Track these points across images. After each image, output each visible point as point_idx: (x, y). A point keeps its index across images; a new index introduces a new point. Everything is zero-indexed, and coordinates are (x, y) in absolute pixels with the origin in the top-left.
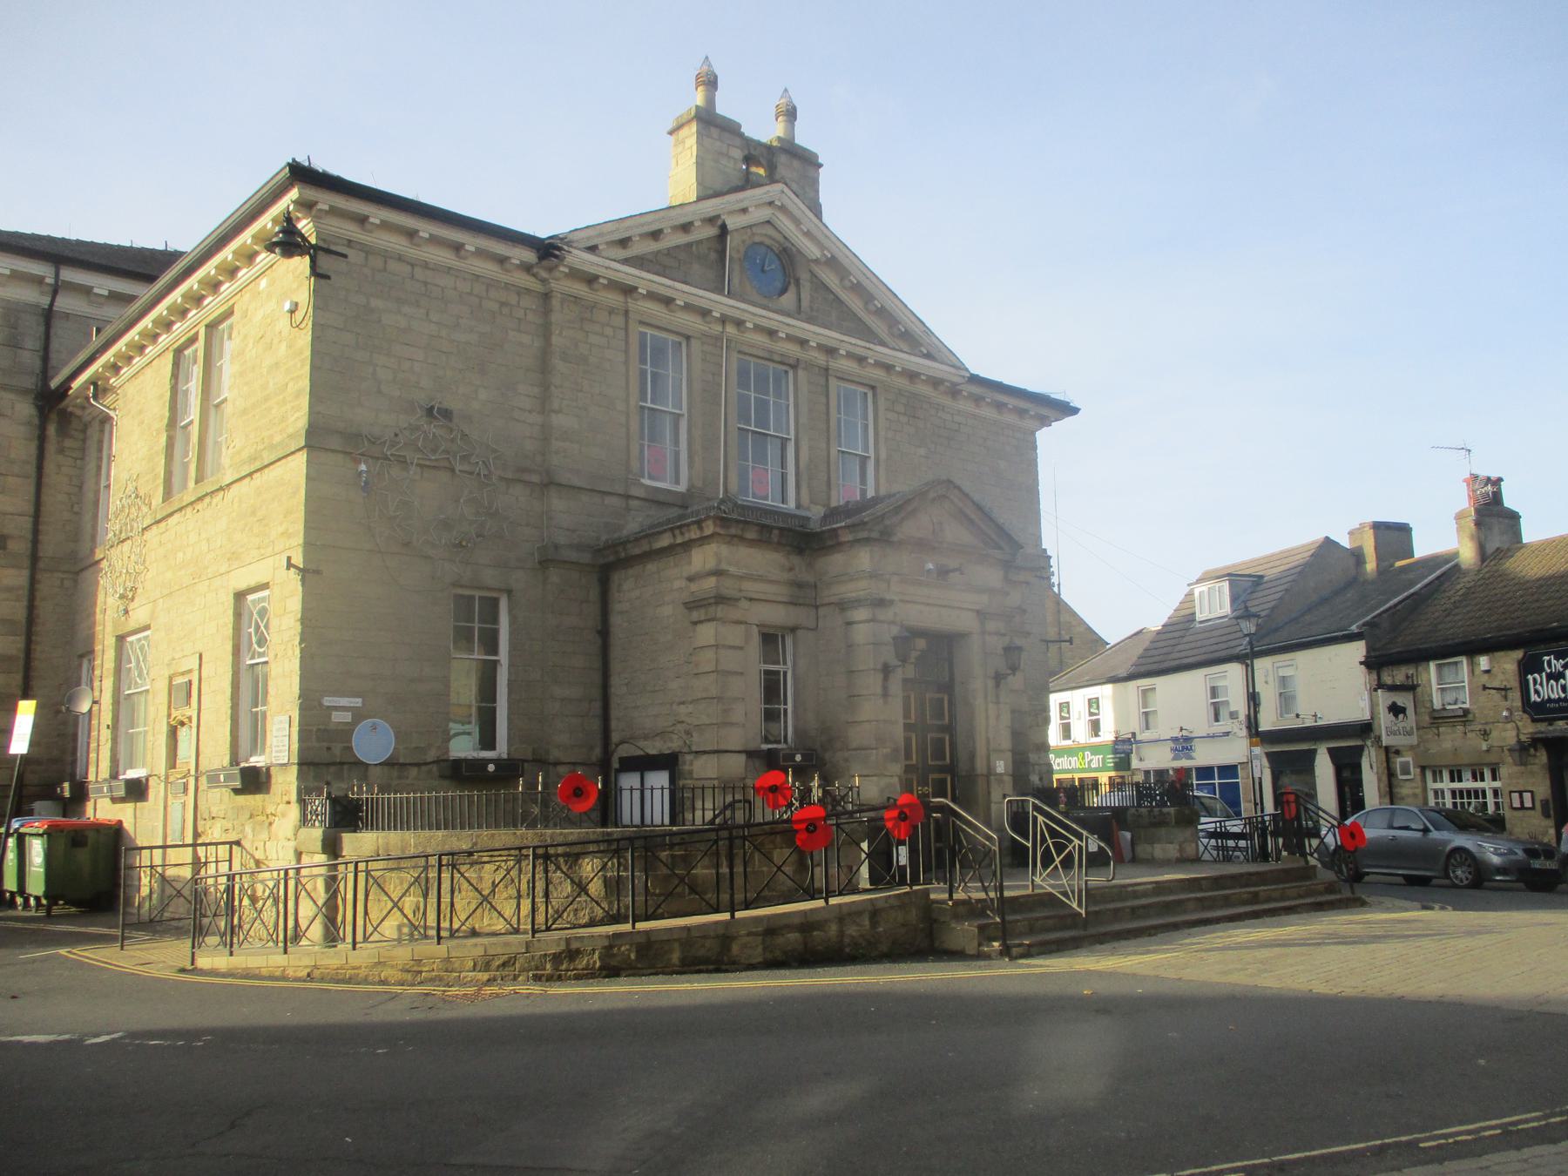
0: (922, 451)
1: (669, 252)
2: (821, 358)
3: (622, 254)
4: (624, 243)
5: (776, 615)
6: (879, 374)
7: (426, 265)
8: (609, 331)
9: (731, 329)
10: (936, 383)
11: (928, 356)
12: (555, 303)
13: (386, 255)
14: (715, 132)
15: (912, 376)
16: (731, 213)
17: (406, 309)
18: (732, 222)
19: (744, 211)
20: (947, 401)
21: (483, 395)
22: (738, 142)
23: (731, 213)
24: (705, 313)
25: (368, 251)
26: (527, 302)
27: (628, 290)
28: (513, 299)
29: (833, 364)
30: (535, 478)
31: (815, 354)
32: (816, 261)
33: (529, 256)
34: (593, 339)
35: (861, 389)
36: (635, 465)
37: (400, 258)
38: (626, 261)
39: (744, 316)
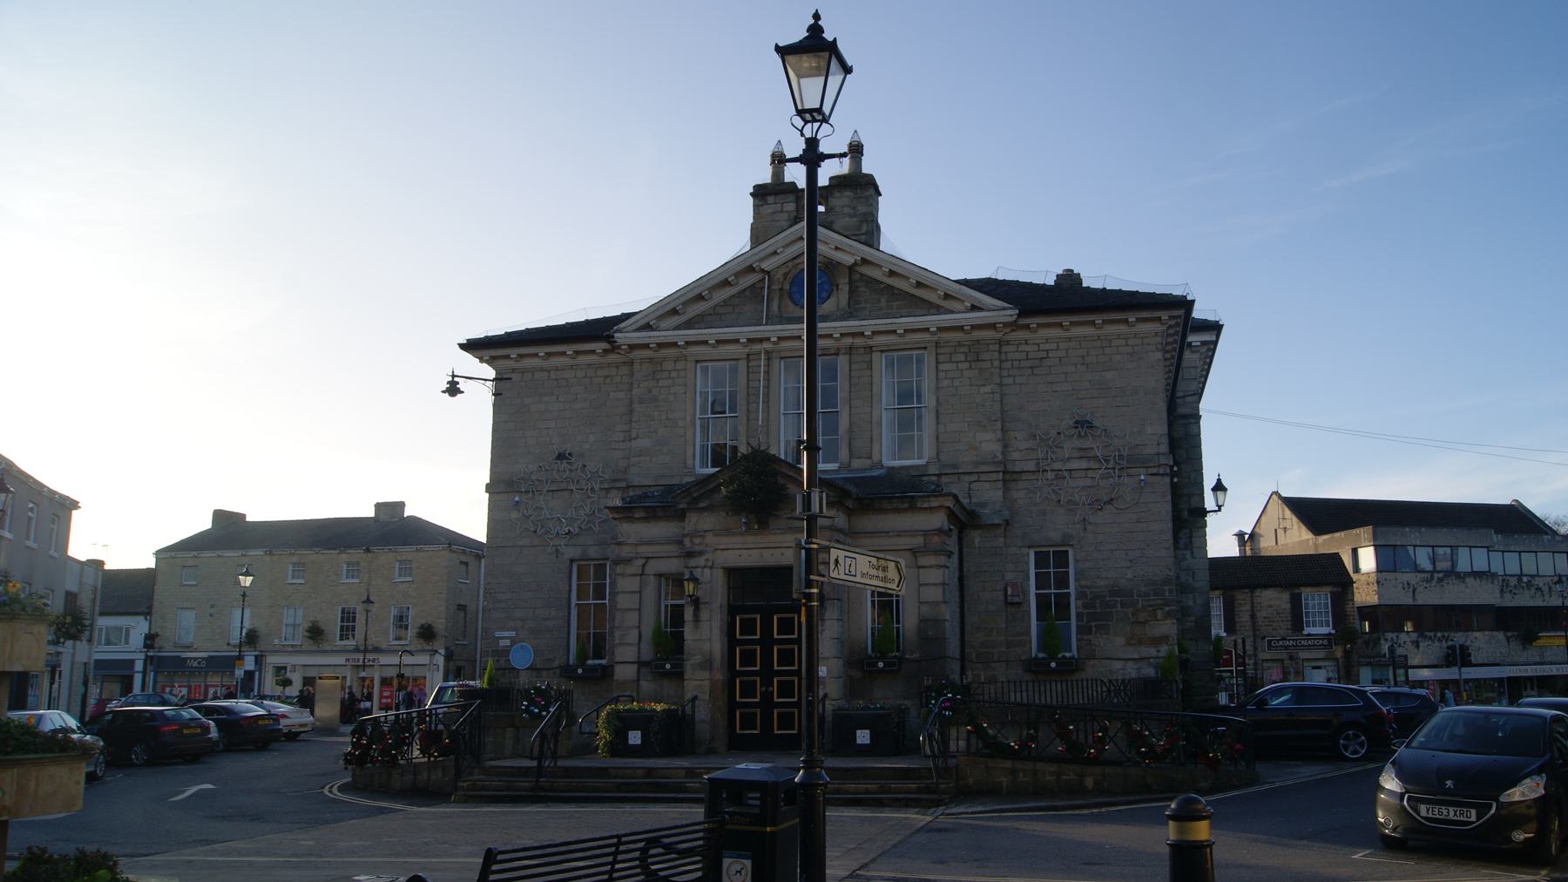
0: (988, 389)
1: (725, 303)
2: (859, 341)
3: (676, 320)
4: (674, 312)
5: (672, 566)
6: (926, 336)
7: (557, 369)
8: (674, 374)
9: (766, 345)
10: (993, 326)
11: (974, 308)
12: (637, 367)
13: (533, 370)
14: (771, 199)
15: (961, 328)
16: (762, 259)
17: (546, 399)
18: (766, 265)
19: (775, 253)
20: (1021, 335)
21: (592, 438)
22: (791, 197)
23: (762, 259)
24: (737, 341)
25: (523, 371)
26: (624, 370)
27: (675, 345)
28: (613, 371)
29: (870, 342)
30: (623, 484)
31: (849, 341)
32: (856, 264)
33: (604, 345)
34: (662, 383)
35: (915, 353)
36: (690, 462)
37: (542, 370)
38: (688, 325)
39: (767, 335)
